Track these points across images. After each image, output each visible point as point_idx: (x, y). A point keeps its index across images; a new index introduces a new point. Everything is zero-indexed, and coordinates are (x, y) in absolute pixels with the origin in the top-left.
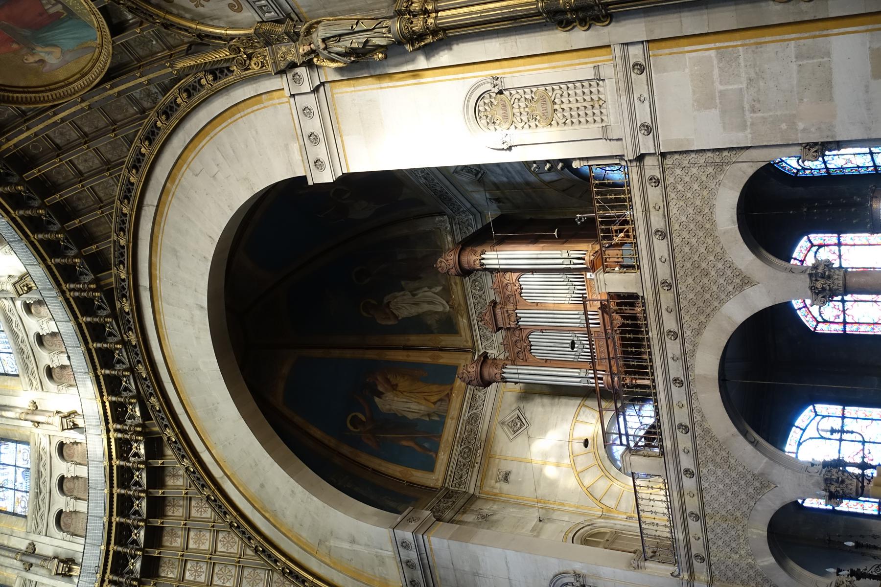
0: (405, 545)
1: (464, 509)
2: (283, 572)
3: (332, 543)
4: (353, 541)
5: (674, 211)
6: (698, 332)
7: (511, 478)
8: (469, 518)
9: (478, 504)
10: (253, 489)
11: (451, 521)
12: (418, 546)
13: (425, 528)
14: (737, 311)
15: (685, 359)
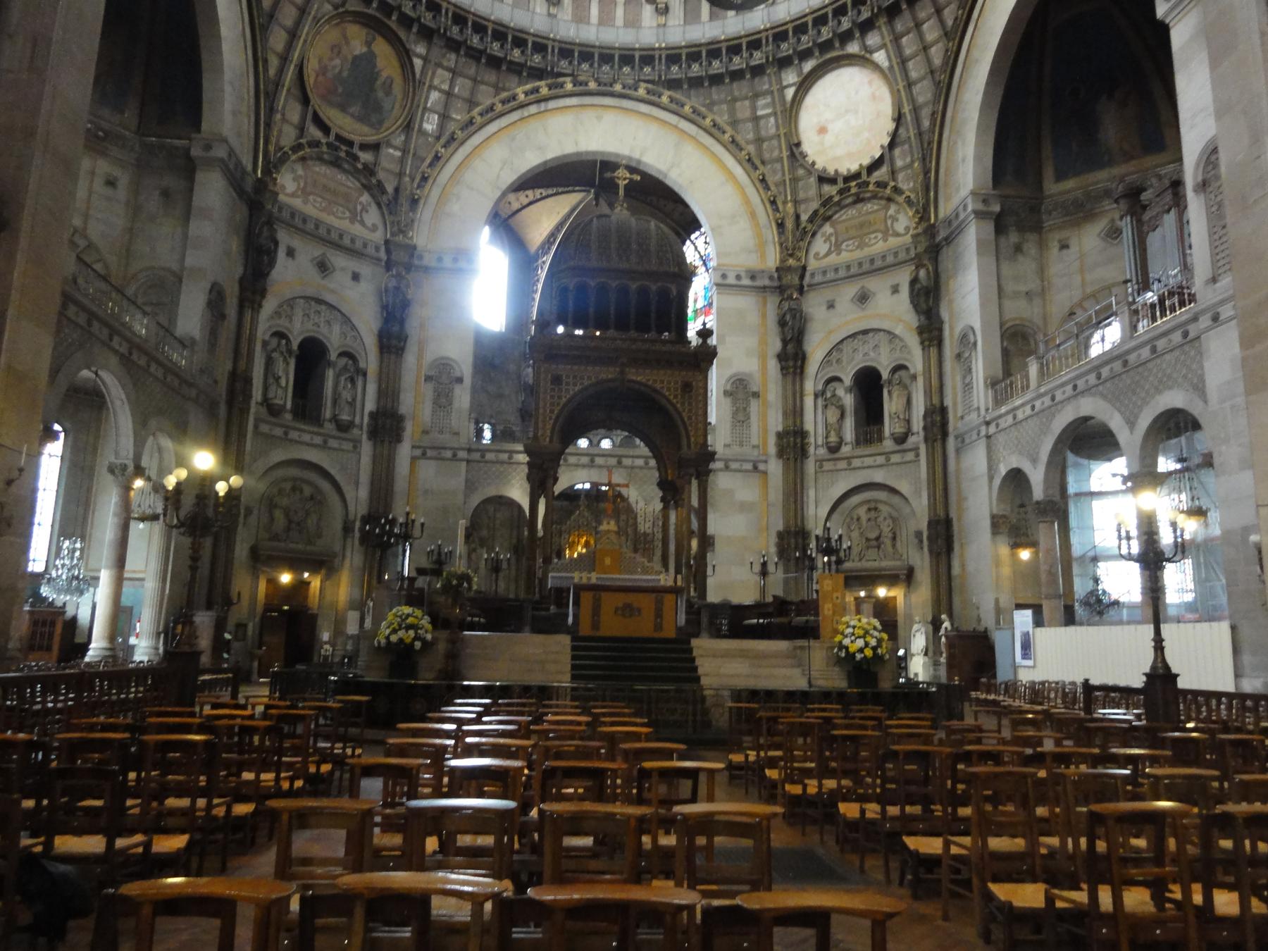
0: (965, 207)
1: (1021, 229)
2: (933, 114)
3: (960, 143)
4: (964, 160)
5: (1167, 357)
6: (1104, 397)
7: (1065, 251)
8: (1014, 237)
9: (1032, 237)
10: (975, 53)
11: (1000, 229)
12: (966, 217)
13: (979, 214)
14: (1116, 423)
15: (1088, 391)
